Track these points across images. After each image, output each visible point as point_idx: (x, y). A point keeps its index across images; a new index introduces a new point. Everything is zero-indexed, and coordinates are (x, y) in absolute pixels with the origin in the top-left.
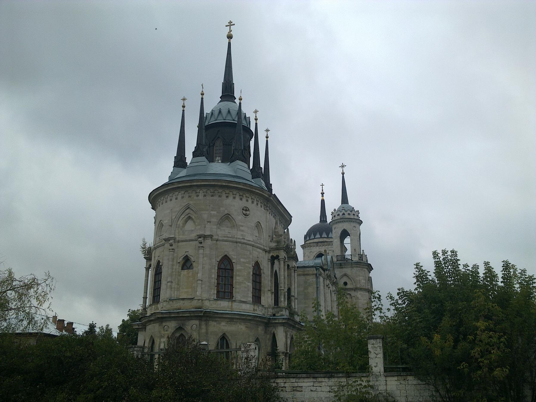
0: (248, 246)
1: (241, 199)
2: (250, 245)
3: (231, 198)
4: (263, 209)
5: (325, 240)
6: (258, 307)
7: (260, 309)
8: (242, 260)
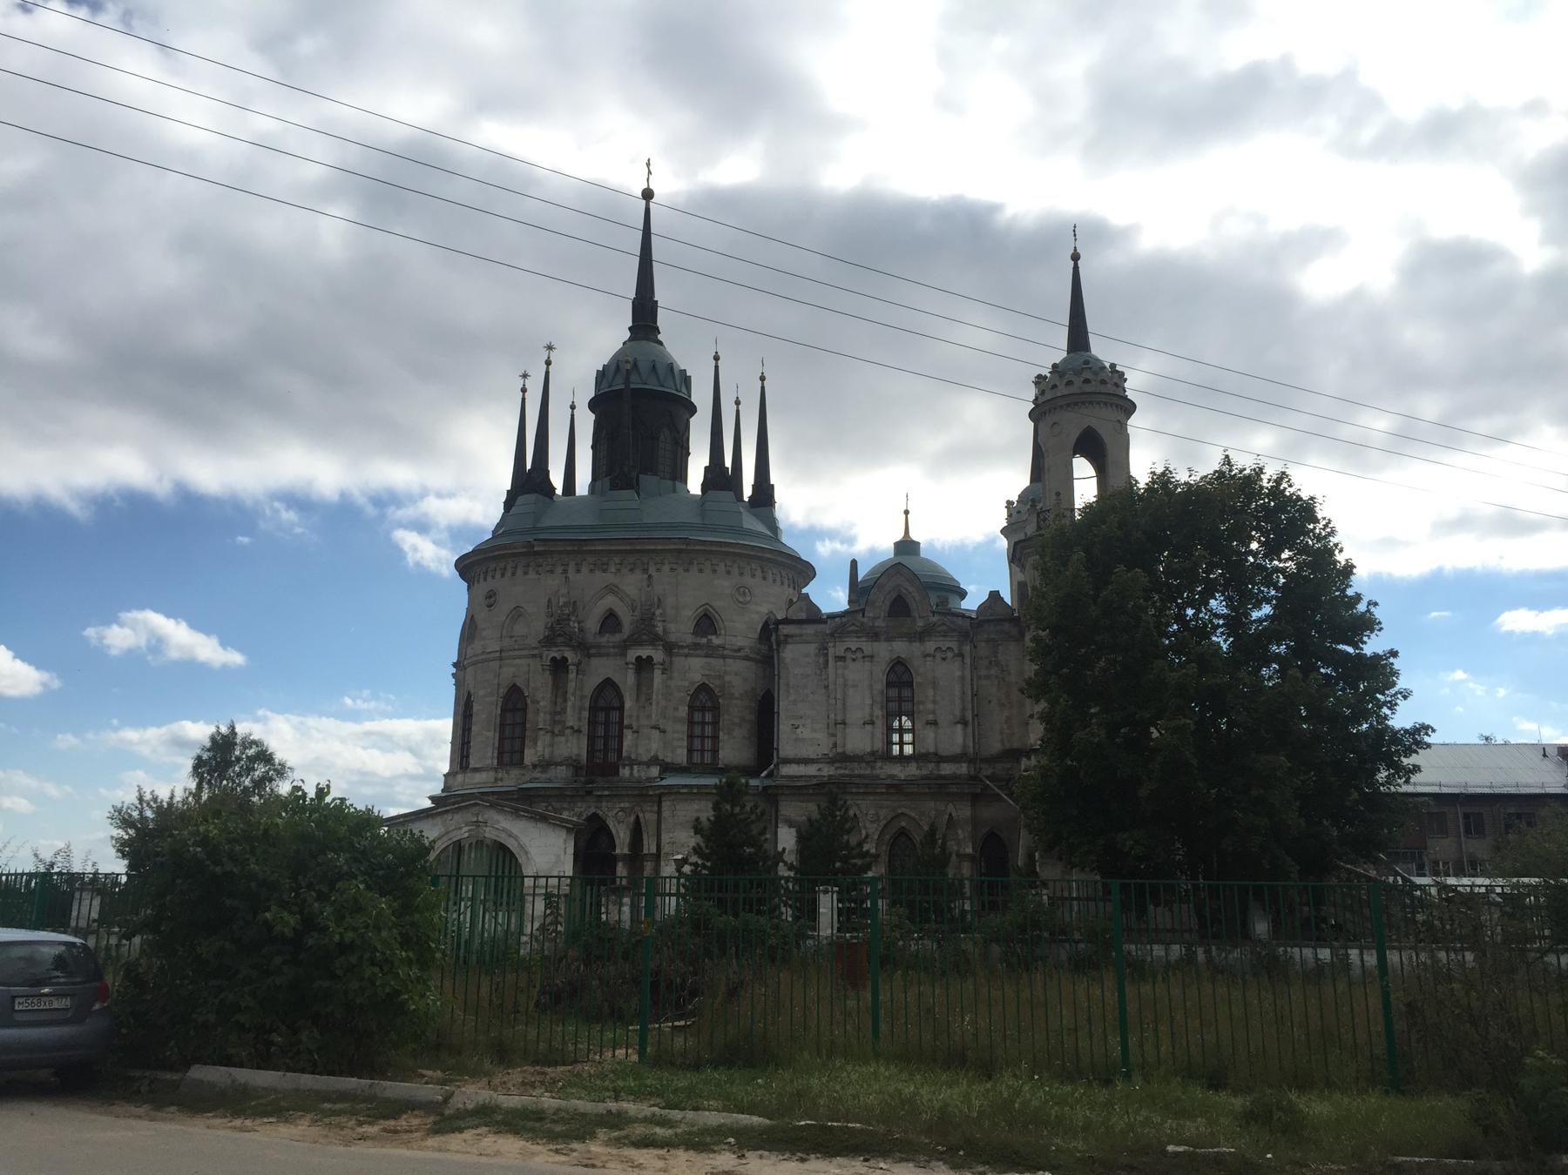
0: (491, 663)
1: (485, 579)
4: (532, 575)
6: (507, 773)
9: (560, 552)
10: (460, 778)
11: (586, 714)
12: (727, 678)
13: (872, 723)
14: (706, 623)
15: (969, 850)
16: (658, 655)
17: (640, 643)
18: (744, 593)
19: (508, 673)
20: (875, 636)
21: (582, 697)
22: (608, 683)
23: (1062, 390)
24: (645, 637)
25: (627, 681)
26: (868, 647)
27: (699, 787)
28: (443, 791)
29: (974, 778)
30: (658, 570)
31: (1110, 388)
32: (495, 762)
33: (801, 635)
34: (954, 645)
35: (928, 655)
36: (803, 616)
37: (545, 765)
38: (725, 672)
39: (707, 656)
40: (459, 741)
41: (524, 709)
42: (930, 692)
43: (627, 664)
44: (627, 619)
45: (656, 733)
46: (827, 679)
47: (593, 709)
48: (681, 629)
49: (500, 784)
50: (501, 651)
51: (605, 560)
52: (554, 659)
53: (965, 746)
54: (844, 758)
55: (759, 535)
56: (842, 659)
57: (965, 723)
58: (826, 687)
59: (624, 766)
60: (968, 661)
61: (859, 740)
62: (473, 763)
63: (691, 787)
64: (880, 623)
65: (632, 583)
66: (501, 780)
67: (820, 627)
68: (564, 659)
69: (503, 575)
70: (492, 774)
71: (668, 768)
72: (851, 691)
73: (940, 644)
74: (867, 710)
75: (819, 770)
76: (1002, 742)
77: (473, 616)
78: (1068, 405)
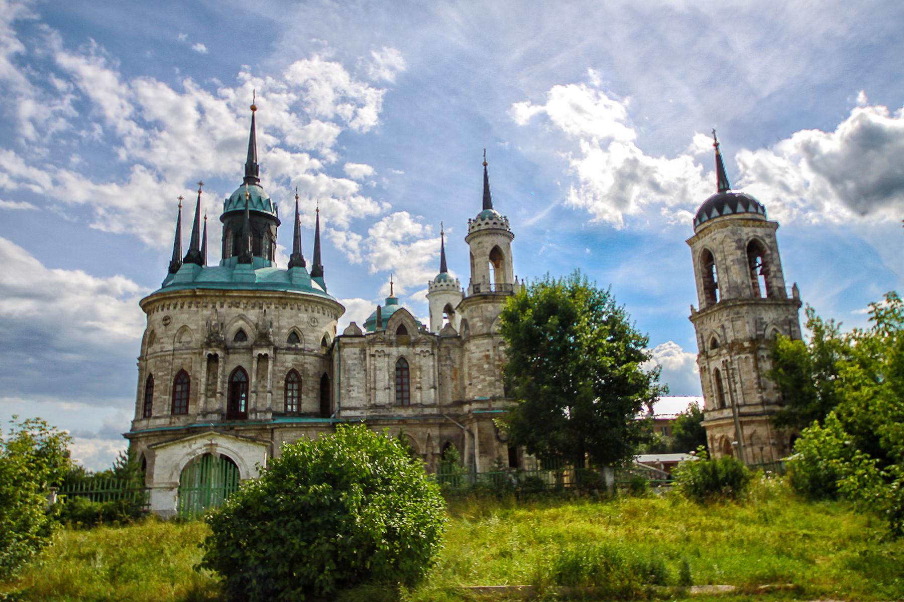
1: (162, 310)
2: (169, 355)
3: (155, 312)
4: (194, 308)
5: (706, 224)
6: (178, 419)
7: (181, 420)
8: (160, 374)
9: (211, 296)
10: (144, 422)
11: (226, 385)
12: (306, 366)
13: (389, 388)
14: (295, 336)
15: (438, 451)
16: (270, 353)
17: (261, 346)
18: (314, 322)
19: (178, 362)
20: (390, 344)
21: (224, 376)
22: (240, 368)
23: (483, 227)
24: (263, 343)
25: (252, 368)
26: (387, 350)
27: (297, 423)
28: (131, 430)
29: (440, 415)
30: (268, 308)
31: (505, 227)
32: (170, 413)
33: (352, 343)
34: (430, 349)
35: (417, 354)
36: (353, 333)
37: (205, 413)
38: (305, 363)
39: (296, 354)
40: (142, 401)
41: (189, 383)
42: (418, 373)
43: (253, 358)
44: (251, 334)
45: (269, 395)
46: (366, 366)
47: (231, 382)
48: (281, 340)
49: (173, 425)
50: (174, 350)
51: (237, 301)
52: (210, 355)
53: (435, 400)
54: (375, 407)
55: (315, 290)
56: (373, 356)
57: (435, 388)
58: (365, 370)
59: (251, 413)
60: (436, 357)
61: (383, 397)
62: (154, 414)
63: (292, 424)
64: (393, 338)
65: (253, 315)
66: (174, 423)
67: (362, 339)
68: (216, 355)
69: (175, 308)
70: (167, 421)
71: (276, 415)
72: (378, 372)
73: (423, 349)
74: (387, 382)
75: (362, 413)
76: (453, 398)
77: (153, 331)
78: (487, 234)
